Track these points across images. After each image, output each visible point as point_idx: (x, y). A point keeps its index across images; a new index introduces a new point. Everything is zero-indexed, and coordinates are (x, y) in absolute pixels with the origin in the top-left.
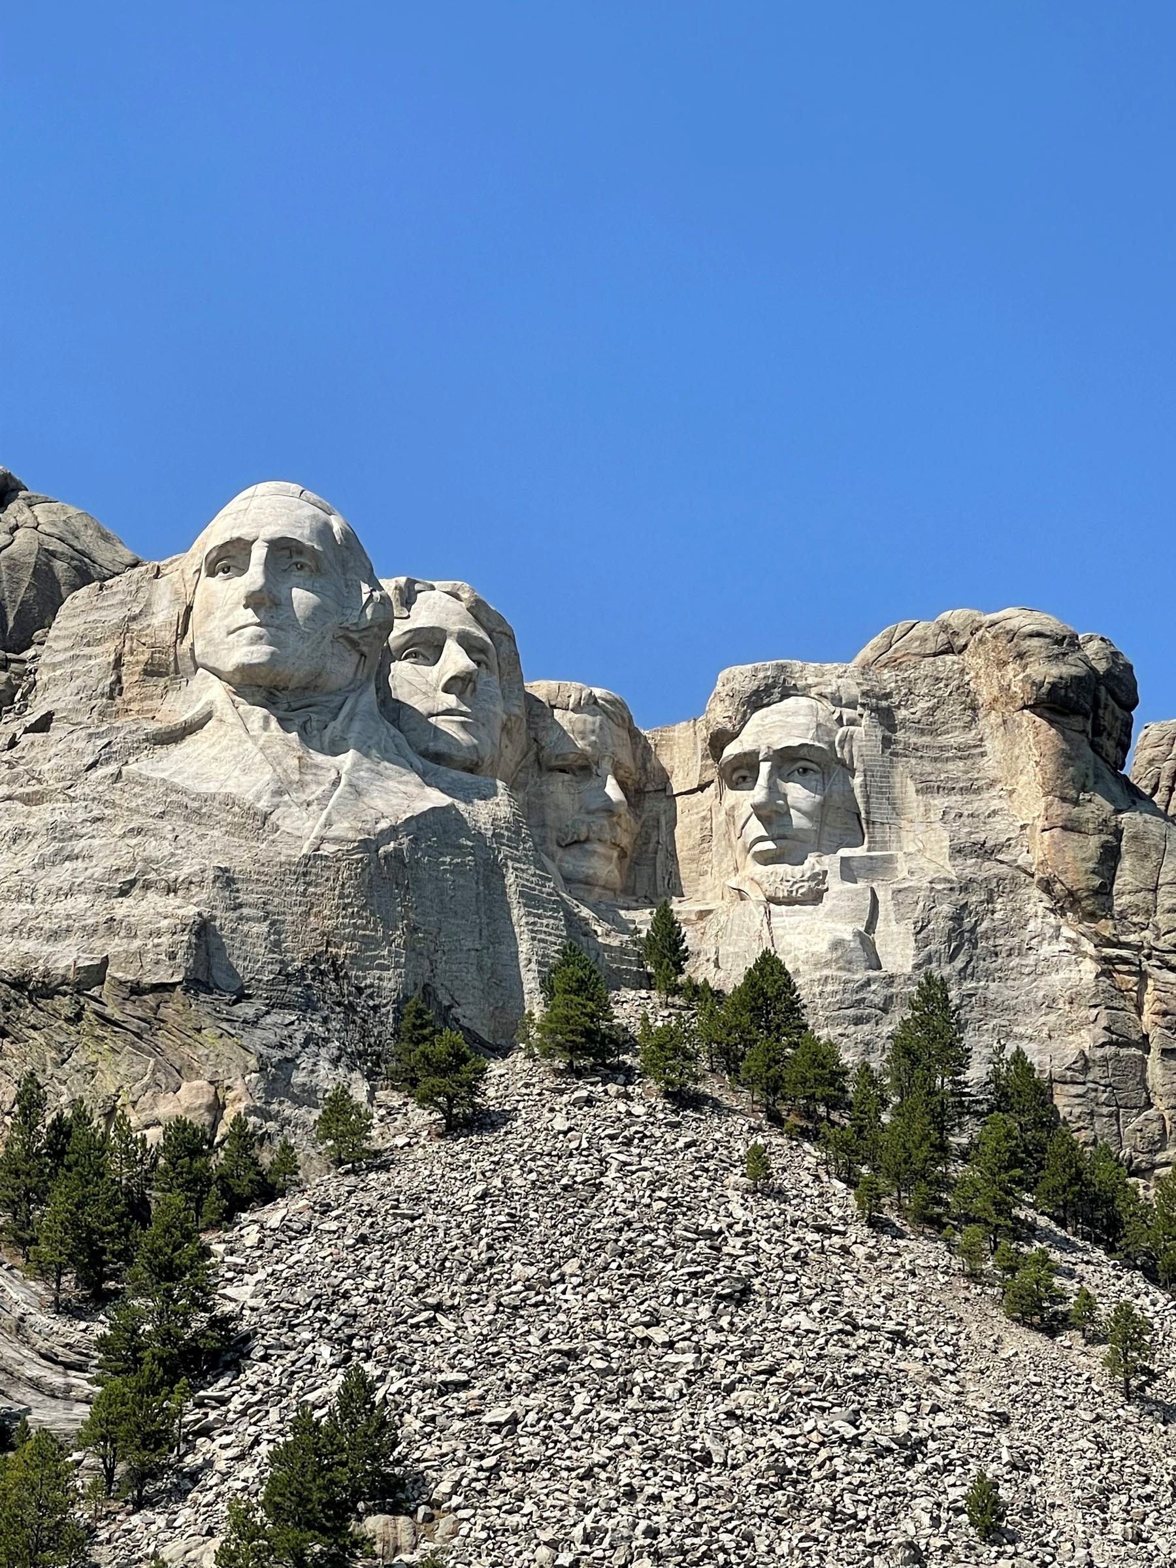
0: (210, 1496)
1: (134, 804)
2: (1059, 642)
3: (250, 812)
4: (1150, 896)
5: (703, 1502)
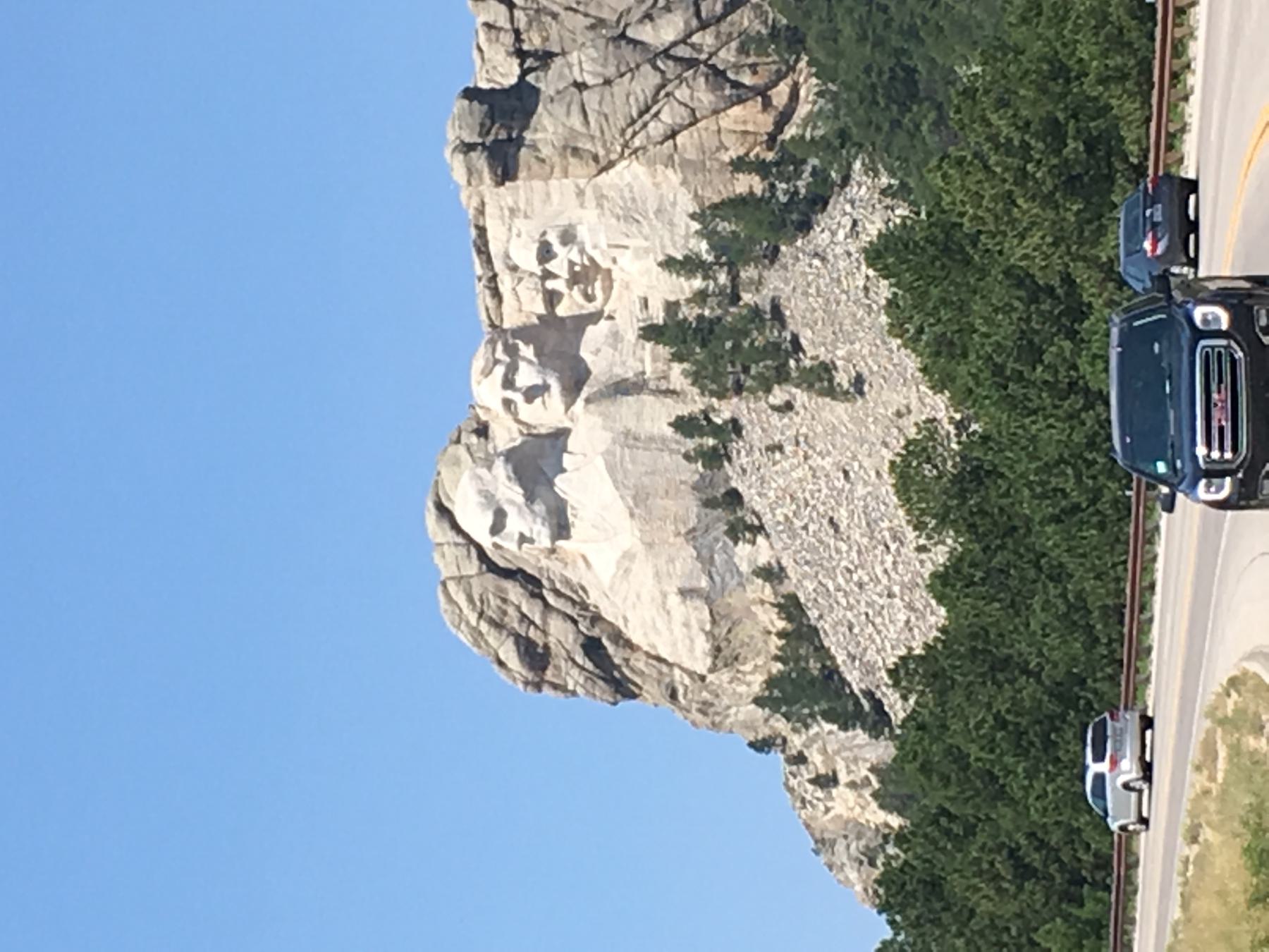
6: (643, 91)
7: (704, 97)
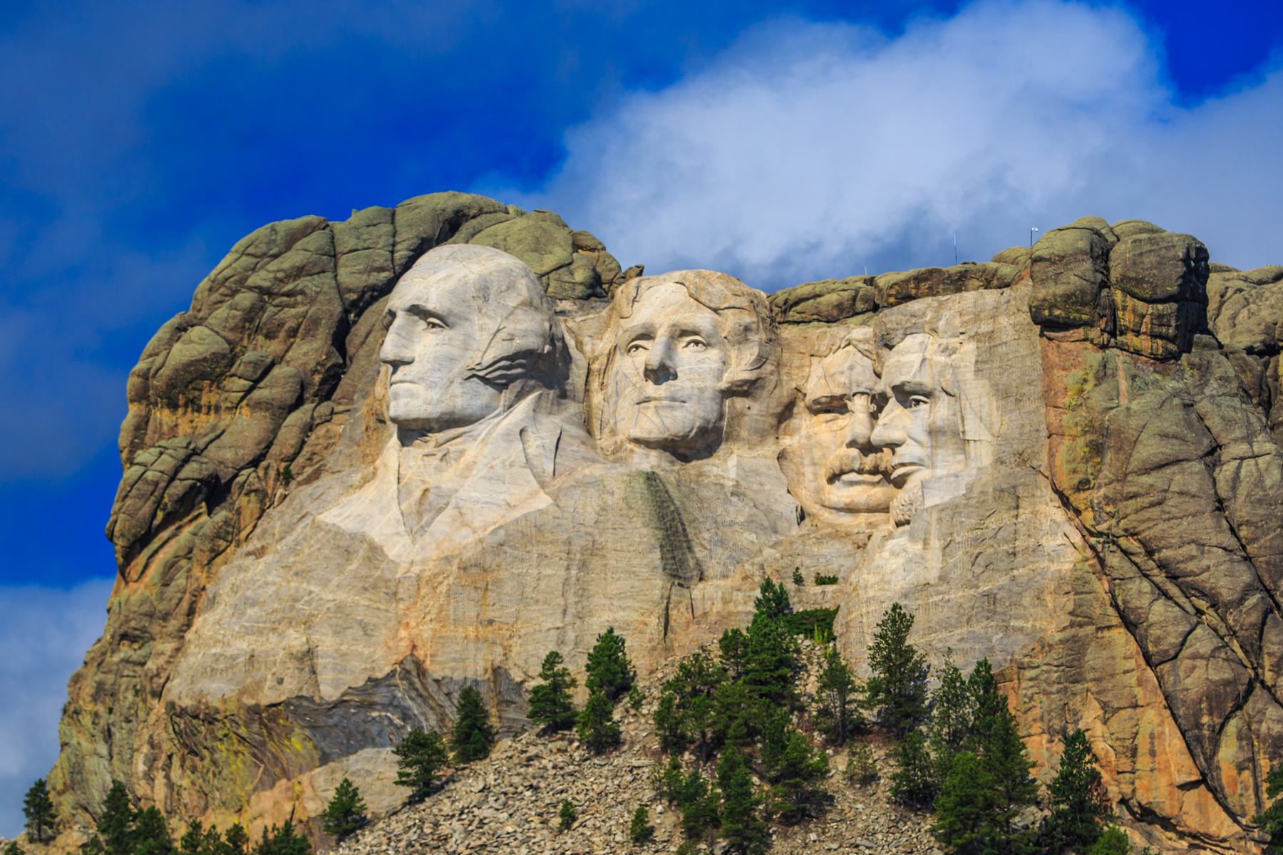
2: (1054, 263)
6: (1208, 568)
7: (1195, 678)
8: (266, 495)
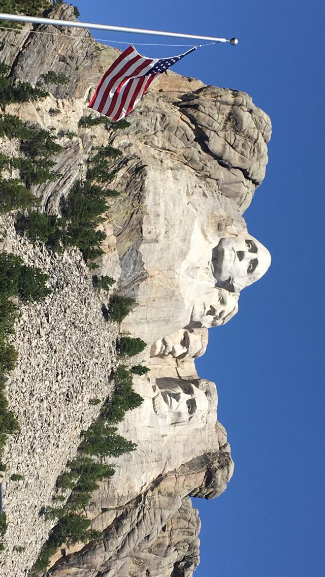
0: (21, 249)
1: (187, 221)
2: (226, 477)
3: (186, 253)
4: (158, 506)
5: (22, 394)
6: (130, 547)
8: (201, 171)
